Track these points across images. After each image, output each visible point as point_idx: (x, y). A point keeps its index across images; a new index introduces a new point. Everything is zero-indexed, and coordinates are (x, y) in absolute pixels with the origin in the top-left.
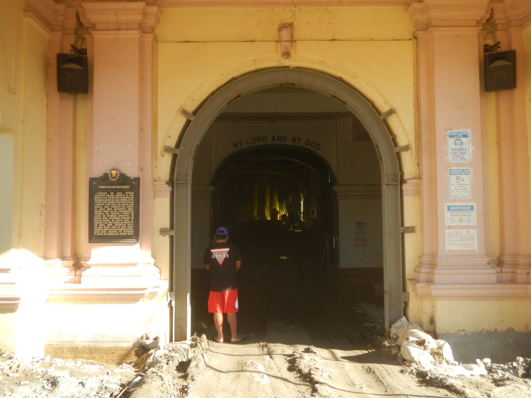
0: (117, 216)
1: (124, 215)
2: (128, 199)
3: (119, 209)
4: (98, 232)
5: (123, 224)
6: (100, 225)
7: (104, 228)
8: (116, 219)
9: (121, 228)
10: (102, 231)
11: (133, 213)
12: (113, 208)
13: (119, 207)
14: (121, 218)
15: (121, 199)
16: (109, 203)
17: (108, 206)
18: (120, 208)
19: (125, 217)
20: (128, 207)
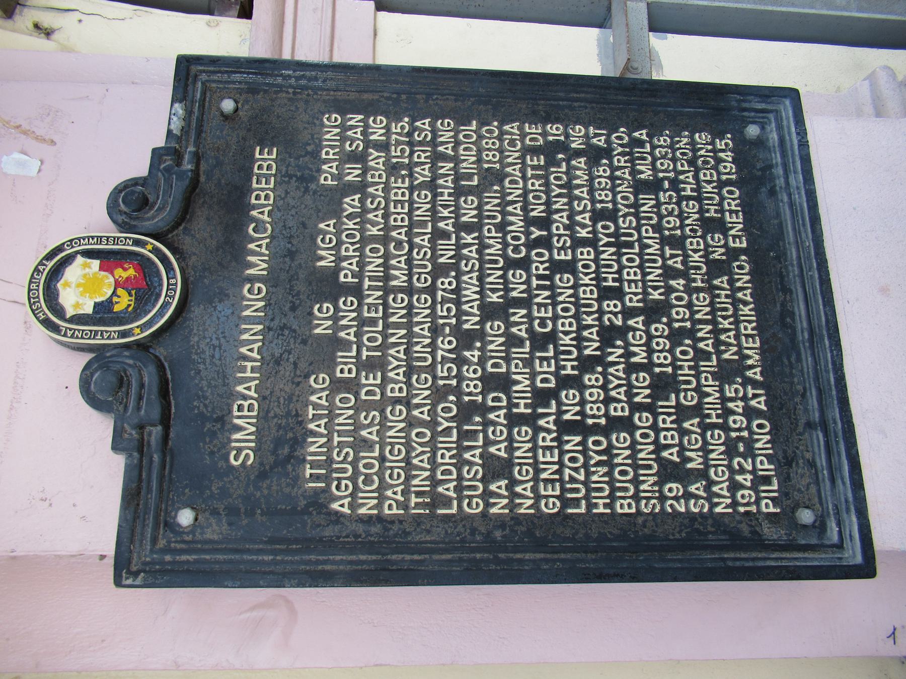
0: (569, 267)
1: (549, 211)
2: (393, 169)
3: (495, 249)
4: (742, 471)
5: (636, 215)
7: (698, 410)
8: (598, 279)
9: (678, 243)
10: (725, 428)
12: (488, 312)
13: (471, 252)
14: (583, 233)
15: (387, 228)
16: (433, 345)
17: (461, 362)
18: (482, 247)
20: (468, 165)
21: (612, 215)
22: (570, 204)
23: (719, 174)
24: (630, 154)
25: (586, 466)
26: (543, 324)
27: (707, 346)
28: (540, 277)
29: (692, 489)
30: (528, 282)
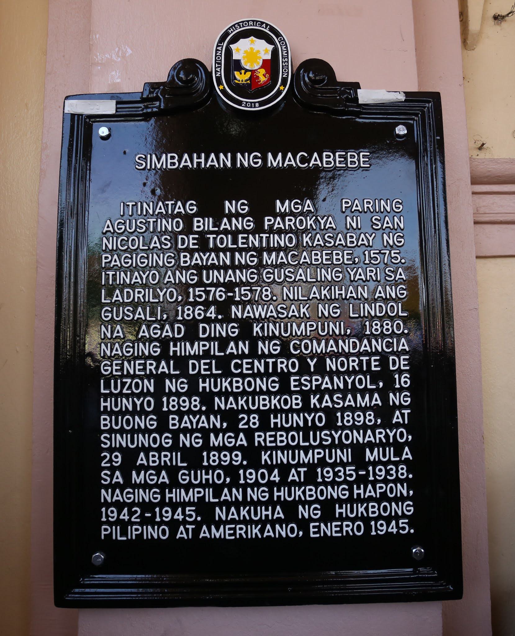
0: (285, 389)
1: (331, 374)
4: (131, 514)
5: (333, 446)
6: (141, 460)
7: (174, 484)
8: (276, 412)
10: (162, 504)
11: (403, 362)
14: (314, 401)
16: (217, 285)
17: (207, 304)
19: (344, 392)
21: (331, 424)
22: (339, 390)
23: (376, 519)
24: (388, 444)
25: (133, 394)
26: (237, 366)
27: (225, 495)
28: (275, 364)
29: (118, 473)
30: (271, 356)
